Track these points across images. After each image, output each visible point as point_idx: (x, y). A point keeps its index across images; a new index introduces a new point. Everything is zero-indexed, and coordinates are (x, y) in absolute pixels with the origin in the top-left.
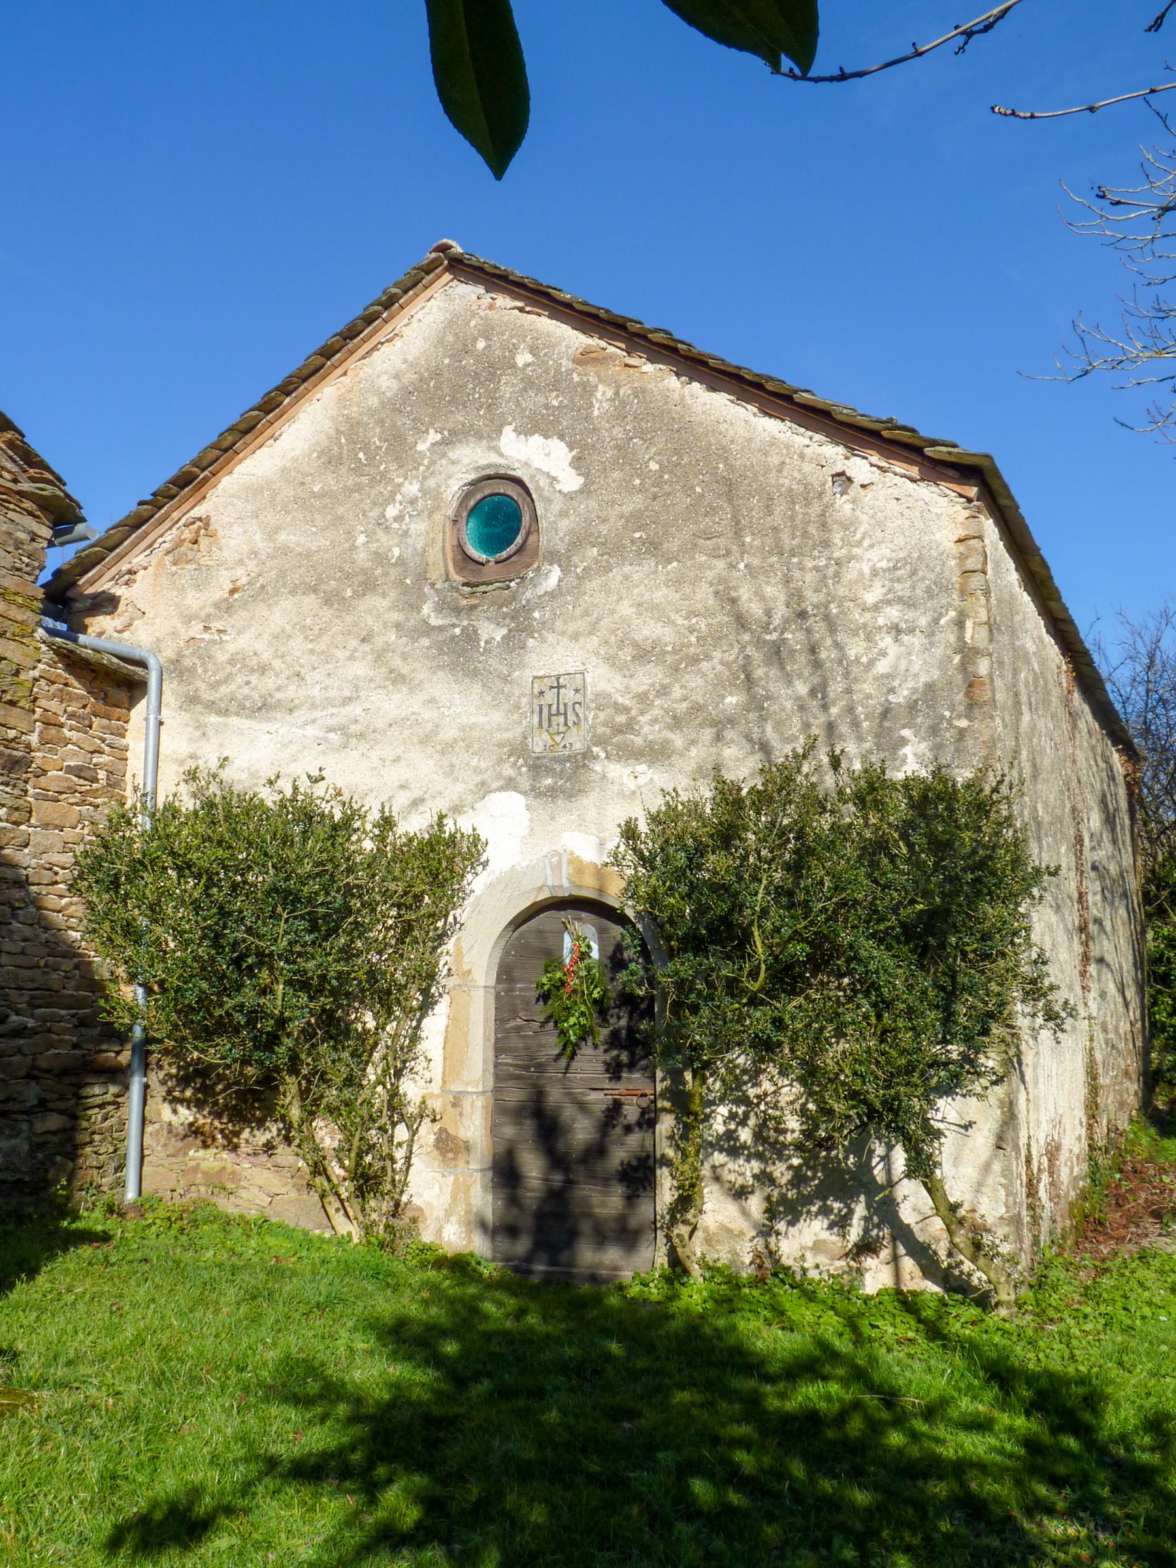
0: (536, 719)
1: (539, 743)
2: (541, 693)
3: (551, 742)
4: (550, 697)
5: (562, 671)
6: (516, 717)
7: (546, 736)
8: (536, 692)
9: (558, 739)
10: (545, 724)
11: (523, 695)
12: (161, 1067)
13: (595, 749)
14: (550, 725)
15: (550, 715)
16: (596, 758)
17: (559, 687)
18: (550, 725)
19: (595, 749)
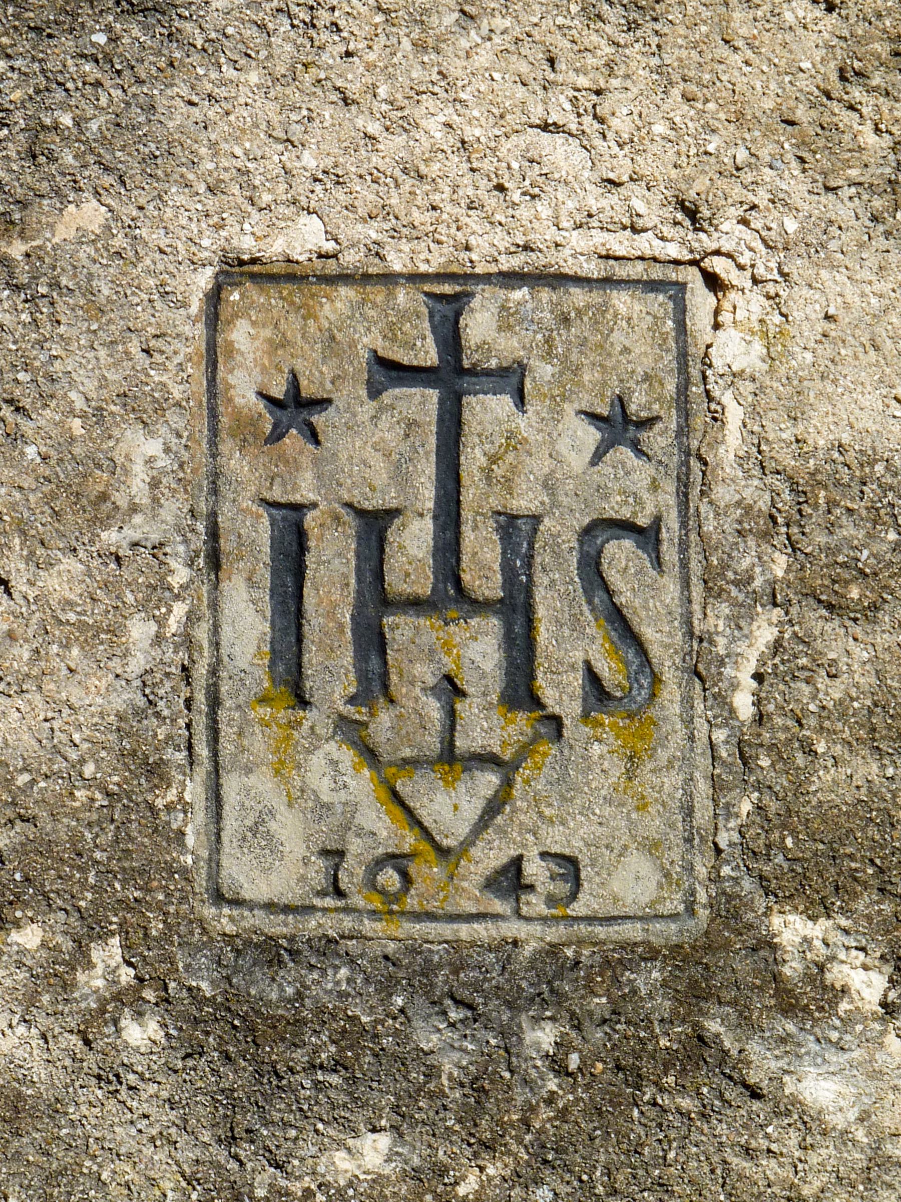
0: (246, 622)
1: (277, 823)
2: (296, 408)
3: (381, 827)
4: (375, 448)
5: (488, 247)
6: (64, 579)
7: (332, 772)
8: (244, 388)
9: (451, 807)
10: (332, 671)
11: (142, 407)
12: (94, 416)
13: (792, 929)
14: (375, 682)
15: (376, 599)
16: (809, 1000)
17: (454, 375)
18: (375, 685)
19: (792, 929)
